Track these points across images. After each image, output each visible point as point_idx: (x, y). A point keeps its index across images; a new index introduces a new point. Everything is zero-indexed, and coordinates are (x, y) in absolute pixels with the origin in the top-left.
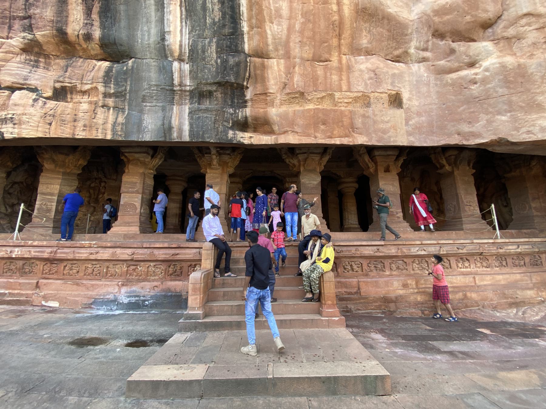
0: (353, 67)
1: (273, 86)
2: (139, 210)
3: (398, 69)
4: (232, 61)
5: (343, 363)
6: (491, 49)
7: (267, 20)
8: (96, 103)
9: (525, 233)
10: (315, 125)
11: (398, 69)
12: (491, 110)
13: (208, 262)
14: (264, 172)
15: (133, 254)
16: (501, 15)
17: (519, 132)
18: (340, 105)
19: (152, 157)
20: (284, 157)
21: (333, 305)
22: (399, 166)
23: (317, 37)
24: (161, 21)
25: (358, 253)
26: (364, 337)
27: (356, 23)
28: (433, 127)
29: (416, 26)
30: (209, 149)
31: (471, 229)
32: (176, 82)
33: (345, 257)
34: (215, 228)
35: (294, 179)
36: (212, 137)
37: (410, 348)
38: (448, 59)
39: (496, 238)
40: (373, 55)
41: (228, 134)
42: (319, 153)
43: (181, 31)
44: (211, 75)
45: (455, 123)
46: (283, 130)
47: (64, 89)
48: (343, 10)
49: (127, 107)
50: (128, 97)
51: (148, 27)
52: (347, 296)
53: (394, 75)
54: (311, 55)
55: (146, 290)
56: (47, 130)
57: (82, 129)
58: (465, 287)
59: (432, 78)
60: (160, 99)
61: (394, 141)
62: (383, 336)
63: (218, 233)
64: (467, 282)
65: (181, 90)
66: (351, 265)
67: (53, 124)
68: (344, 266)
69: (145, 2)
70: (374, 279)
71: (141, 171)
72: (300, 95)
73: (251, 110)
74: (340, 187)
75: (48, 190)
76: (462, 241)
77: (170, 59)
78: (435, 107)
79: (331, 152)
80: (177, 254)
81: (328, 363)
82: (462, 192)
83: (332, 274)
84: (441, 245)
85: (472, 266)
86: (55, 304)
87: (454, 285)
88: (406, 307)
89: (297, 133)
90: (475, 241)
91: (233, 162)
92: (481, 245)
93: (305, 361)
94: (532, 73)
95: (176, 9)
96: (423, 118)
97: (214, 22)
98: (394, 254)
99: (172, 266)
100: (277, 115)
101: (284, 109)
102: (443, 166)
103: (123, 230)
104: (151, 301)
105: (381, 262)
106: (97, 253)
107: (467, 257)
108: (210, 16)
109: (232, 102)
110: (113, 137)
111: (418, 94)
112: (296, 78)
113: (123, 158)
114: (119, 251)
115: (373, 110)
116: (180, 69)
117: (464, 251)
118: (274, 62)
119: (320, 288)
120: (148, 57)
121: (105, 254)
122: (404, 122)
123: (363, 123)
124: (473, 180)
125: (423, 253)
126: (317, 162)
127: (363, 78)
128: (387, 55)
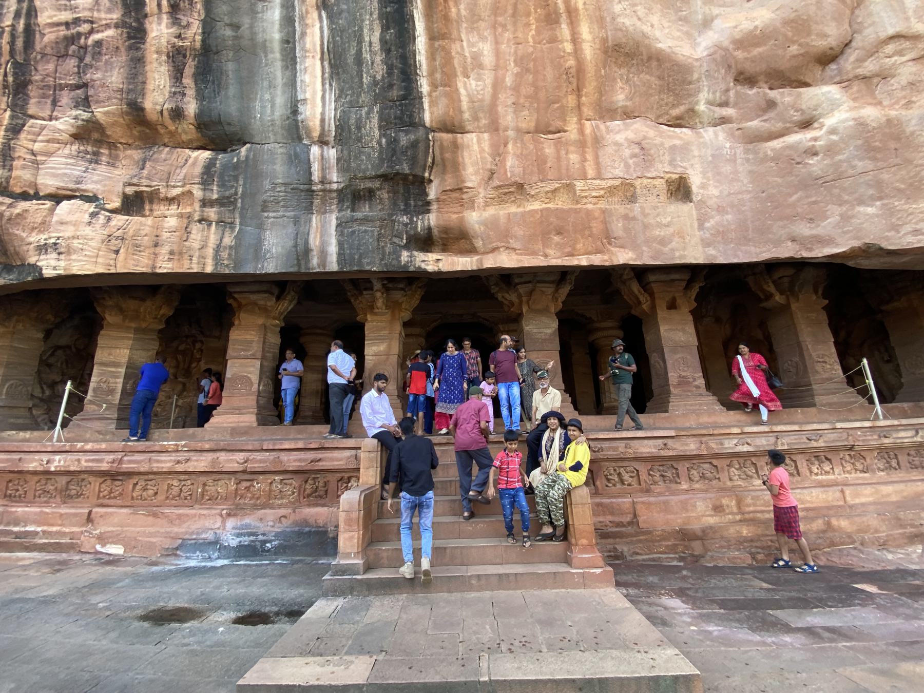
0: (603, 139)
1: (472, 176)
2: (256, 386)
3: (680, 138)
4: (404, 140)
5: (615, 653)
6: (838, 96)
7: (459, 74)
8: (189, 216)
10: (545, 237)
11: (680, 138)
12: (846, 197)
13: (372, 472)
14: (464, 315)
15: (246, 462)
16: (850, 41)
17: (898, 232)
18: (585, 201)
19: (278, 298)
20: (494, 289)
21: (590, 545)
22: (693, 297)
23: (542, 95)
24: (292, 84)
25: (630, 453)
26: (650, 604)
27: (604, 68)
28: (747, 231)
29: (705, 68)
30: (370, 282)
31: (830, 405)
32: (316, 177)
33: (608, 460)
34: (382, 413)
35: (512, 326)
36: (374, 262)
37: (734, 624)
38: (765, 118)
39: (876, 418)
40: (635, 117)
41: (400, 256)
42: (552, 282)
43: (323, 97)
44: (372, 165)
45: (786, 222)
46: (490, 246)
47: (139, 196)
48: (582, 50)
49: (238, 221)
50: (239, 205)
51: (271, 94)
52: (614, 529)
53: (673, 148)
54: (533, 124)
55: (269, 522)
56: (112, 262)
57: (166, 258)
59: (740, 150)
60: (291, 206)
62: (683, 602)
63: (386, 422)
64: (830, 499)
65: (324, 190)
66: (619, 474)
67: (122, 251)
68: (606, 476)
69: (266, 56)
70: (661, 498)
71: (260, 321)
72: (517, 188)
73: (437, 216)
74: (592, 338)
75: (112, 358)
76: (815, 426)
77: (305, 142)
78: (749, 196)
79: (573, 278)
80: (320, 460)
81: (587, 653)
83: (586, 491)
84: (778, 435)
85: (836, 471)
86: (116, 550)
87: (808, 505)
88: (722, 547)
89: (515, 250)
90: (839, 425)
91: (409, 302)
92: (851, 432)
93: (545, 650)
94: (912, 133)
95: (314, 65)
96: (729, 217)
97: (374, 81)
98: (694, 453)
99: (310, 482)
101: (491, 211)
102: (769, 296)
103: (230, 420)
104: (276, 542)
105: (673, 466)
106: (188, 460)
107: (826, 454)
108: (367, 73)
109: (407, 205)
110: (216, 268)
111: (718, 177)
112: (510, 162)
113: (230, 301)
114: (223, 456)
115: (641, 207)
116: (322, 156)
117: (821, 443)
118: (472, 140)
119: (565, 516)
120: (272, 140)
121: (201, 463)
122: (696, 225)
123: (626, 230)
124: (826, 317)
125: (746, 448)
126: (550, 297)
127: (621, 156)
128: (659, 117)
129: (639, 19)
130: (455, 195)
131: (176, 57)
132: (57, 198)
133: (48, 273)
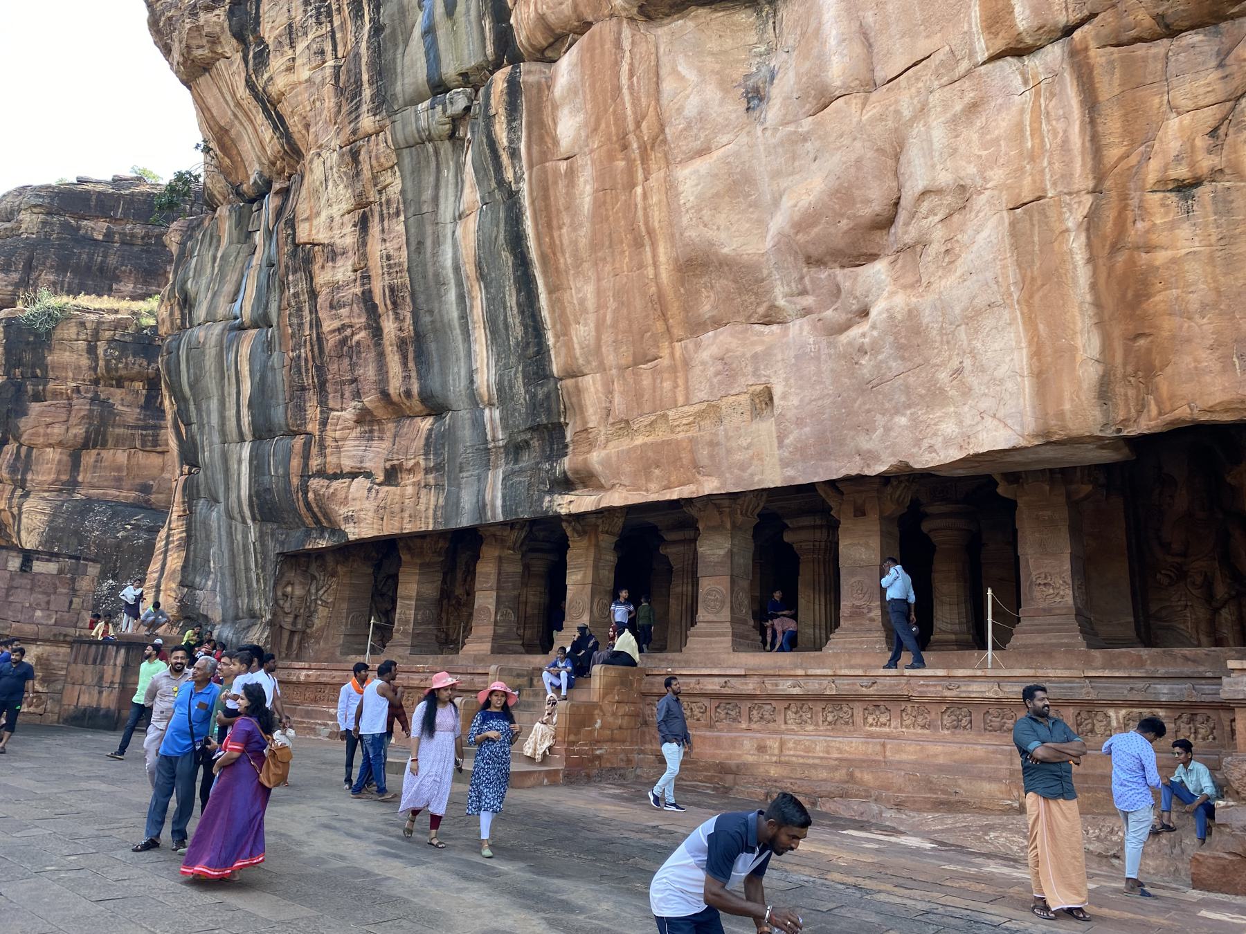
1: (593, 417)
3: (763, 342)
4: (541, 393)
9: (1186, 658)
18: (678, 429)
23: (635, 327)
27: (683, 285)
32: (489, 438)
47: (393, 467)
58: (864, 761)
61: (760, 481)
82: (1028, 552)
87: (845, 756)
96: (807, 429)
100: (601, 463)
102: (996, 484)
109: (552, 450)
115: (725, 430)
117: (872, 691)
122: (776, 444)
123: (712, 457)
125: (797, 691)
129: (705, 226)
130: (584, 435)
131: (402, 344)
132: (353, 475)
133: (351, 537)
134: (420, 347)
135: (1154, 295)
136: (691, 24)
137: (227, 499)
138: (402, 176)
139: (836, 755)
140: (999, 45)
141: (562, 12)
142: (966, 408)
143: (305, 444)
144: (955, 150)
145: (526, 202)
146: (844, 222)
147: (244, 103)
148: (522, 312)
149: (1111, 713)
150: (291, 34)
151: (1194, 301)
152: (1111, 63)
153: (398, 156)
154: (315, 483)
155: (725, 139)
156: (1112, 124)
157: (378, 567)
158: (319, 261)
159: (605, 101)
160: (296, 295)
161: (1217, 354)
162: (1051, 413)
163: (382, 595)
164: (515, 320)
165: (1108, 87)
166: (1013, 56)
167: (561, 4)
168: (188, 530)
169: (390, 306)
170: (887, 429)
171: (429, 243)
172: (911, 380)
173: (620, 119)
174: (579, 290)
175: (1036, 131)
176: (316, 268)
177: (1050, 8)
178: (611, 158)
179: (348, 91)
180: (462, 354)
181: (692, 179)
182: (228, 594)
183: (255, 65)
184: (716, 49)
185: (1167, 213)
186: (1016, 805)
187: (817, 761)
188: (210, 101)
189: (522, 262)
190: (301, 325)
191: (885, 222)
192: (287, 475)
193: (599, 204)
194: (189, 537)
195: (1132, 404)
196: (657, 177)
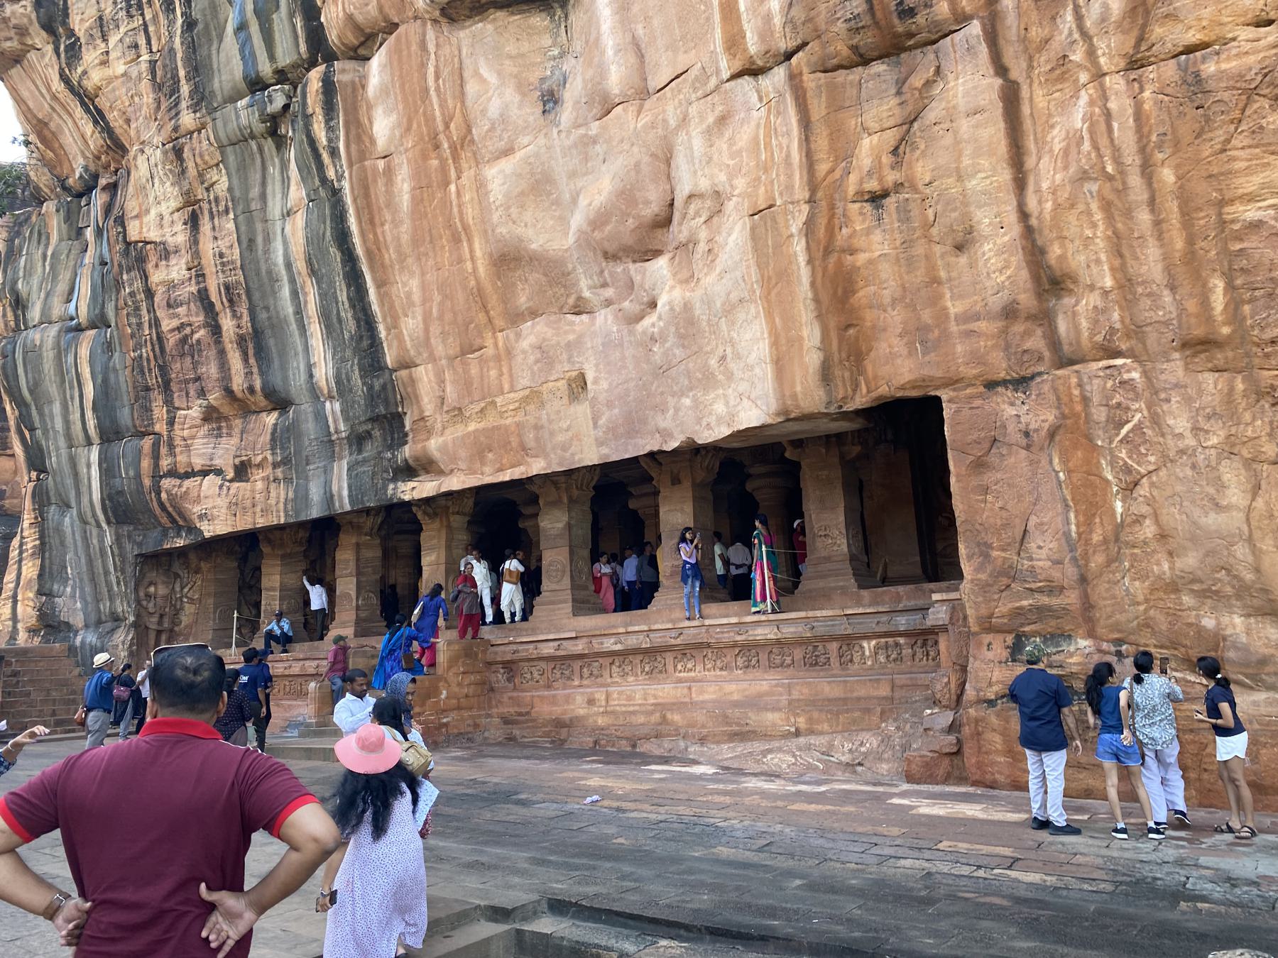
1: (428, 405)
3: (574, 331)
23: (460, 318)
25: (535, 654)
27: (499, 279)
32: (332, 430)
33: (521, 660)
47: (242, 463)
53: (569, 344)
58: (674, 704)
82: (810, 506)
85: (698, 668)
87: (660, 701)
96: (616, 411)
100: (439, 450)
109: (392, 439)
114: (308, 663)
117: (678, 641)
123: (537, 439)
125: (618, 647)
129: (514, 223)
130: (422, 423)
131: (241, 341)
132: (204, 473)
133: (207, 535)
134: (260, 343)
135: (857, 291)
136: (490, 27)
137: (79, 503)
138: (229, 174)
139: (652, 701)
140: (738, 65)
141: (368, 12)
142: (730, 391)
143: (154, 444)
144: (711, 159)
145: (348, 200)
146: (631, 220)
147: (60, 96)
148: (353, 306)
149: (865, 644)
150: (102, 27)
151: (887, 295)
152: (819, 87)
153: (222, 153)
154: (166, 483)
155: (526, 140)
156: (821, 143)
157: (244, 560)
158: (153, 259)
159: (415, 102)
160: (132, 294)
161: (905, 340)
162: (787, 394)
163: (250, 587)
164: (347, 315)
165: (818, 109)
166: (749, 75)
167: (367, 5)
168: (42, 537)
169: (226, 304)
170: (677, 410)
171: (260, 240)
172: (691, 365)
173: (430, 119)
174: (405, 285)
175: (768, 145)
176: (150, 267)
177: (772, 35)
178: (425, 157)
179: (165, 87)
180: (300, 348)
181: (499, 177)
182: (89, 599)
183: (67, 58)
184: (514, 52)
185: (864, 221)
186: (793, 730)
187: (637, 708)
188: (25, 94)
189: (349, 257)
190: (140, 325)
191: (664, 222)
192: (138, 476)
193: (417, 202)
194: (43, 544)
195: (848, 384)
196: (468, 175)
